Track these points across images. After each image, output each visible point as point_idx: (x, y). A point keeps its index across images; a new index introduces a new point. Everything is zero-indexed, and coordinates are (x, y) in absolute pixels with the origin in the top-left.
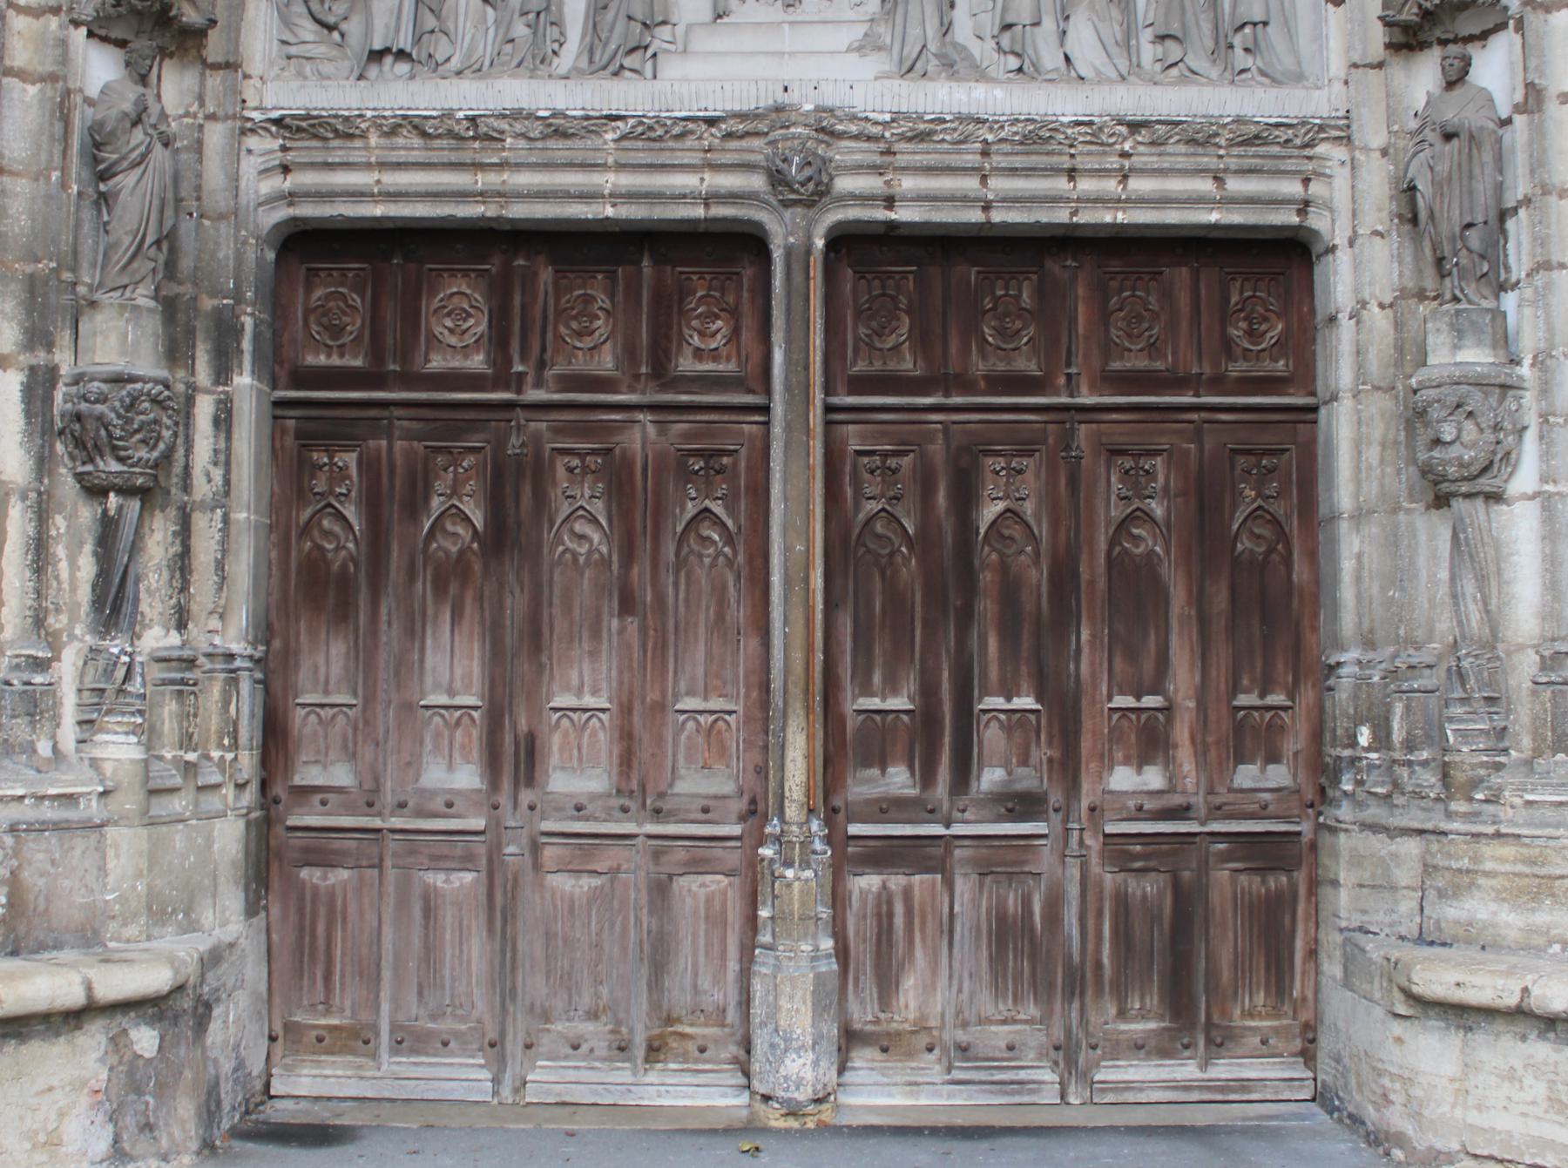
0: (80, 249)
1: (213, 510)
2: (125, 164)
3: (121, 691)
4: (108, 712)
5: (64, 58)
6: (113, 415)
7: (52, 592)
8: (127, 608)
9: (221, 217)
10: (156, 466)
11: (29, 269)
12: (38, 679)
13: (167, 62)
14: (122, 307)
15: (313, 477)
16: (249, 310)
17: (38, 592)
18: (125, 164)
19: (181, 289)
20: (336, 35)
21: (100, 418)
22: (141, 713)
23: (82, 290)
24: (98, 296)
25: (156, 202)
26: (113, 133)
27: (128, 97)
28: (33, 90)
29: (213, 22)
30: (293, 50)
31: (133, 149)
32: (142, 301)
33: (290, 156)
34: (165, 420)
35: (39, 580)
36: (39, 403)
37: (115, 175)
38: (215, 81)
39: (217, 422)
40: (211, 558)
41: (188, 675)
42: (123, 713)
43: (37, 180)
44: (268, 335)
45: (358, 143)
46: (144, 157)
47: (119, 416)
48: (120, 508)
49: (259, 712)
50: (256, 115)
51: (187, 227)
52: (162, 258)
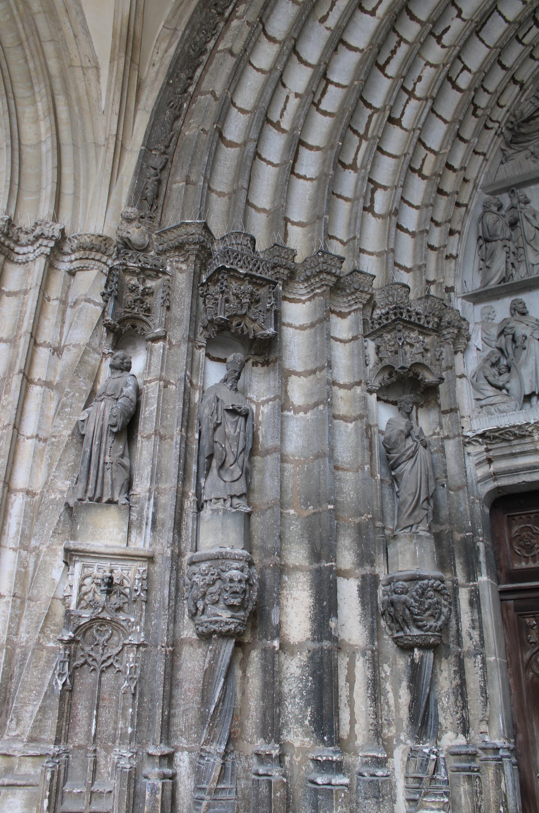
0: (385, 510)
1: (475, 656)
2: (404, 458)
3: (433, 779)
4: (426, 794)
5: (366, 407)
6: (412, 600)
7: (385, 713)
8: (431, 722)
9: (459, 488)
10: (440, 631)
11: (357, 520)
12: (380, 773)
13: (420, 410)
14: (411, 537)
15: (528, 633)
16: (481, 539)
17: (376, 714)
18: (404, 458)
19: (443, 527)
20: (504, 391)
21: (405, 603)
22: (446, 794)
23: (387, 532)
24: (397, 533)
25: (424, 477)
26: (396, 442)
27: (402, 424)
28: (351, 426)
29: (442, 379)
30: (483, 402)
31: (408, 449)
32: (422, 533)
33: (491, 453)
34: (443, 601)
35: (376, 706)
36: (368, 596)
37: (399, 465)
38: (446, 420)
39: (471, 603)
40: (477, 686)
41: (473, 765)
42: (435, 795)
43: (357, 471)
44: (492, 554)
45: (528, 440)
46: (415, 452)
47: (416, 601)
48: (422, 658)
49: (517, 785)
50: (470, 434)
51: (442, 493)
52: (431, 509)
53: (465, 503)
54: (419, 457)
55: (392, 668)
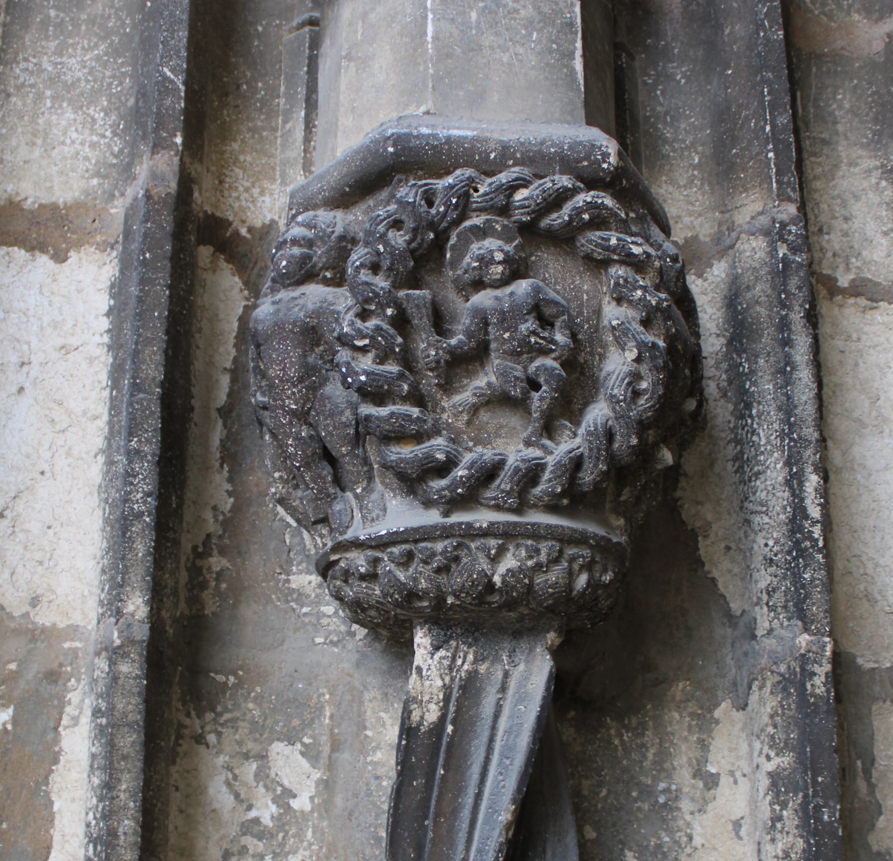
55: (331, 766)
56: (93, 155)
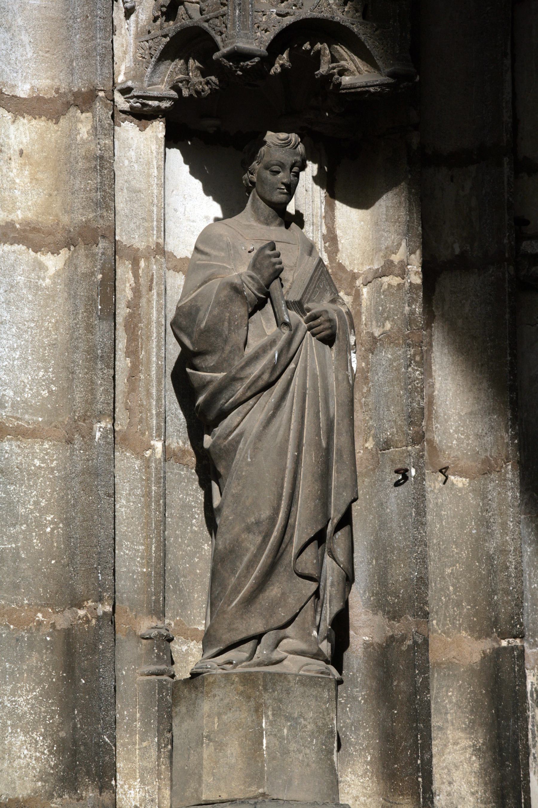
31: (255, 357)
37: (224, 414)
53: (504, 525)
54: (296, 381)
56: (38, 766)
